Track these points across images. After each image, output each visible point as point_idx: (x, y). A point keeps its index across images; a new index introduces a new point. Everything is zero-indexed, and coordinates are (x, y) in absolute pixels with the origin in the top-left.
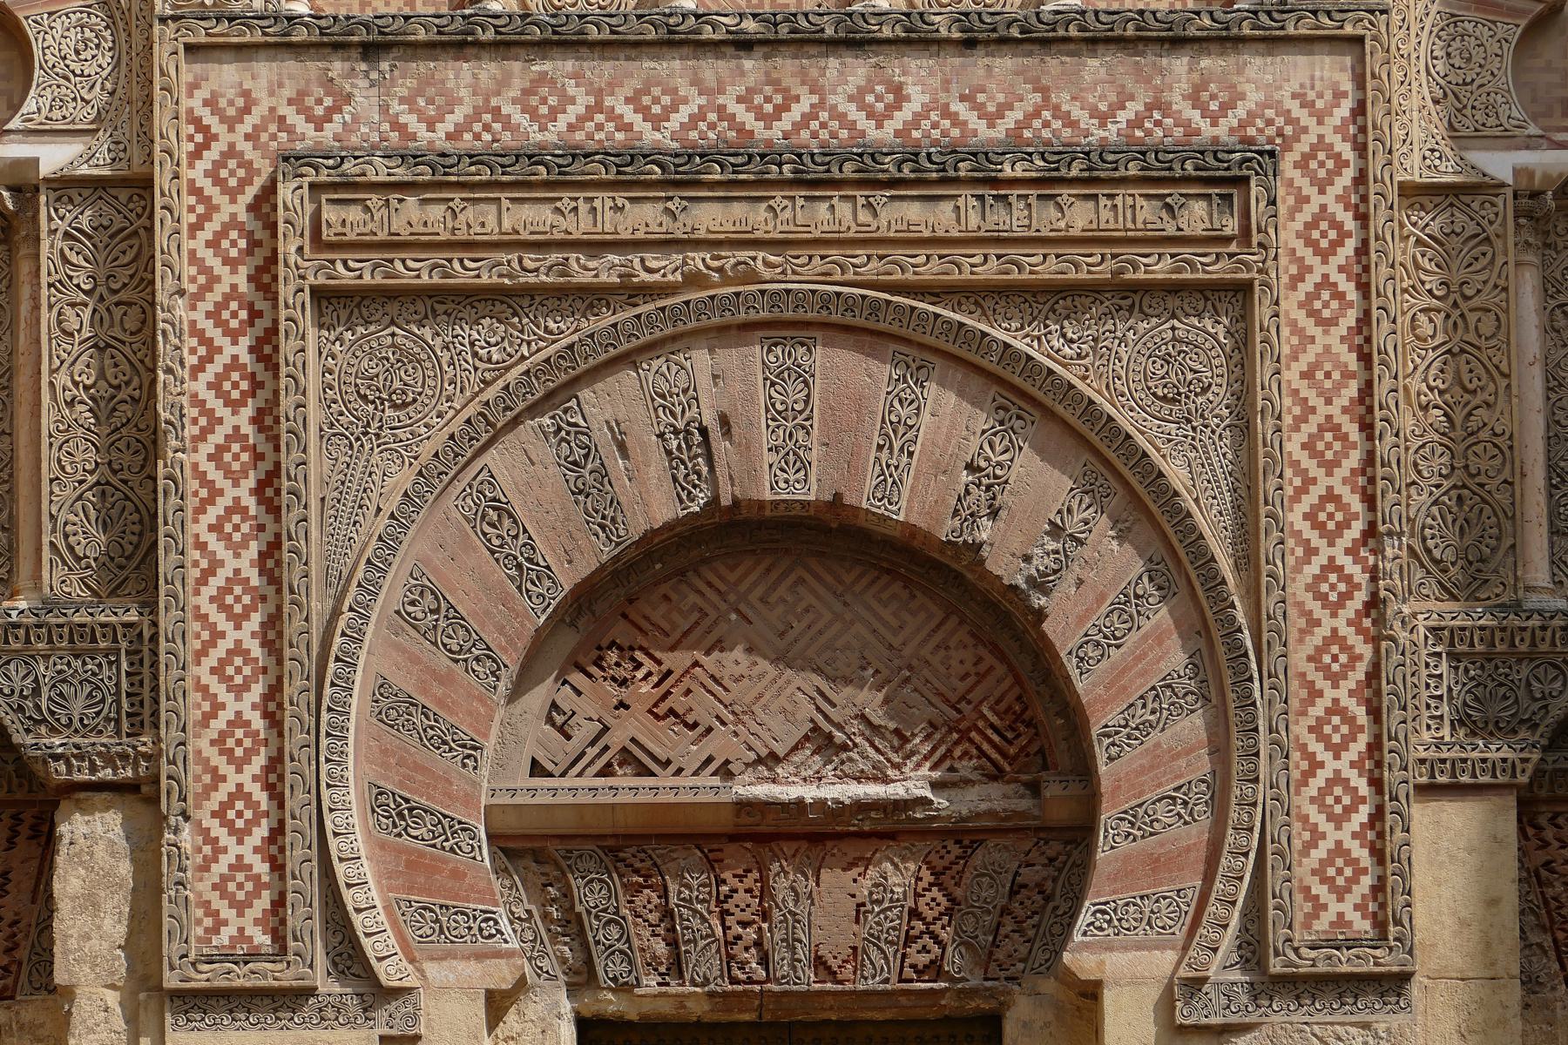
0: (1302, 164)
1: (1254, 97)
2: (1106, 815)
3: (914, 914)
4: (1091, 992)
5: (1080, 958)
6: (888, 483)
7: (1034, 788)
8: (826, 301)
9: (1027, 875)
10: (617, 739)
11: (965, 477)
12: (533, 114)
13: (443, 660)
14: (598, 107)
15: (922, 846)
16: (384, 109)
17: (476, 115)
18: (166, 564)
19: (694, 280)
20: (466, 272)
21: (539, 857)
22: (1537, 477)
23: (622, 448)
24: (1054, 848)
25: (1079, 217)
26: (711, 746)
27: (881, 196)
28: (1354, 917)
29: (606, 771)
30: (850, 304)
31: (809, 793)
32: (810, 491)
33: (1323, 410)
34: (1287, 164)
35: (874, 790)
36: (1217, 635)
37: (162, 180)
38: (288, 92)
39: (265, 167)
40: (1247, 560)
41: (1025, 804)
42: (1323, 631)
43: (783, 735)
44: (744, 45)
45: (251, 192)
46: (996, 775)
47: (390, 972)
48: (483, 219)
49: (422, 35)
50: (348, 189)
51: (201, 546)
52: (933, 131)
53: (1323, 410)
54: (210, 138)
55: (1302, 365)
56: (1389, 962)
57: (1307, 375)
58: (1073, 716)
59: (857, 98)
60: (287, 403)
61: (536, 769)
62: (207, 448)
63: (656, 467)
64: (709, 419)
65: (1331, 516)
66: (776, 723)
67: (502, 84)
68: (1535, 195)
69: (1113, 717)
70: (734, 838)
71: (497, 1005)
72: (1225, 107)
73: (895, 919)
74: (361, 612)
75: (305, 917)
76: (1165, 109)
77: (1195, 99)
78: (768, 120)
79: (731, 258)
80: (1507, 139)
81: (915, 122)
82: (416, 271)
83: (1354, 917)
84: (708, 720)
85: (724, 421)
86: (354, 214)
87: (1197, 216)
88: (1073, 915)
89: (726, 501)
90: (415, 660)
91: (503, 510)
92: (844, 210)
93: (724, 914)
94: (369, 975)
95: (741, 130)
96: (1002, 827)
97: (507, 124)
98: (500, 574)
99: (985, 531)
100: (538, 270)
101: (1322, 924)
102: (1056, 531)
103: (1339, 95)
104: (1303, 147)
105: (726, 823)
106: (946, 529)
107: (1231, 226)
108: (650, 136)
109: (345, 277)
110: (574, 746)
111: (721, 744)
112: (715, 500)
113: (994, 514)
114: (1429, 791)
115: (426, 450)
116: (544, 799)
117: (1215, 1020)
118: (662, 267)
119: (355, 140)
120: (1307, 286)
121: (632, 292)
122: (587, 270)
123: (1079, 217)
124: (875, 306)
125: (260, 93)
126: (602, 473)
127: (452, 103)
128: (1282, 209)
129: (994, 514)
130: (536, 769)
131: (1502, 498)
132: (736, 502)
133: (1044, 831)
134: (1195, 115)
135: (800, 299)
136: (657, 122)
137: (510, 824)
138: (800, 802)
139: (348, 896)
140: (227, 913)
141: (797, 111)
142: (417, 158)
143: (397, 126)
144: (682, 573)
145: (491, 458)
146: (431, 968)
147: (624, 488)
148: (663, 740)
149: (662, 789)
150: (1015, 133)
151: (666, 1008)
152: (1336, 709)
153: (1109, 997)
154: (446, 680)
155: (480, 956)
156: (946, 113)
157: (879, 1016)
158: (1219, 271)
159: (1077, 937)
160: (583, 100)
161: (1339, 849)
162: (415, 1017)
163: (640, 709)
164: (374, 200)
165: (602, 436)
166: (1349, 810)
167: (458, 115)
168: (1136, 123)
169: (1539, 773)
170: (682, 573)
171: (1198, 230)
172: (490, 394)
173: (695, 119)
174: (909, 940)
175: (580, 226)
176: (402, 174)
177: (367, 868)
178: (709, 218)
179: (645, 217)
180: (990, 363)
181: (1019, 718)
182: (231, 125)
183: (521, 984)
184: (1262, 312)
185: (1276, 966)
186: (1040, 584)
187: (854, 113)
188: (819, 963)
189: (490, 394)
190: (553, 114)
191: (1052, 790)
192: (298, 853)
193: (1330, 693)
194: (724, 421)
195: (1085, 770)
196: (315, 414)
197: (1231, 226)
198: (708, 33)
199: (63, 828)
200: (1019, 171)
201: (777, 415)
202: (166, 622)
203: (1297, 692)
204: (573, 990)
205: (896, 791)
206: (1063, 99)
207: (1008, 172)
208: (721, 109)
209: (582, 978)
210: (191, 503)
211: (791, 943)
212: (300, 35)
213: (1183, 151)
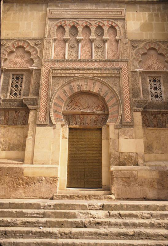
0: (123, 69)
1: (120, 65)
2: (110, 113)
3: (95, 120)
4: (108, 126)
5: (107, 123)
6: (93, 89)
7: (104, 111)
8: (89, 77)
9: (104, 118)
11: (99, 89)
15: (96, 115)
18: (40, 94)
19: (80, 76)
20: (63, 75)
21: (66, 115)
22: (141, 90)
23: (74, 87)
24: (106, 116)
25: (108, 72)
26: (80, 108)
27: (93, 71)
28: (129, 120)
29: (72, 109)
30: (91, 77)
31: (87, 111)
34: (122, 69)
36: (118, 100)
37: (42, 69)
39: (49, 68)
40: (120, 95)
41: (103, 112)
43: (85, 107)
44: (84, 61)
45: (48, 70)
46: (101, 110)
47: (54, 123)
48: (64, 72)
50: (55, 70)
51: (42, 93)
54: (46, 67)
56: (132, 124)
58: (107, 106)
60: (49, 83)
61: (66, 109)
62: (43, 86)
63: (76, 88)
64: (80, 85)
65: (126, 92)
68: (140, 72)
70: (81, 114)
71: (62, 126)
73: (93, 120)
74: (54, 97)
75: (48, 119)
76: (114, 66)
77: (116, 65)
79: (82, 74)
80: (138, 69)
81: (96, 66)
82: (59, 75)
83: (129, 120)
85: (81, 85)
86: (55, 71)
87: (116, 72)
88: (107, 119)
89: (81, 90)
91: (65, 91)
92: (90, 72)
93: (80, 120)
94: (52, 123)
96: (102, 114)
98: (64, 95)
100: (68, 75)
101: (127, 121)
102: (106, 93)
103: (126, 65)
104: (124, 68)
105: (81, 113)
107: (118, 73)
108: (77, 67)
109: (54, 75)
110: (69, 108)
112: (80, 90)
113: (101, 92)
114: (135, 111)
116: (67, 111)
117: (118, 128)
118: (77, 75)
120: (124, 77)
121: (75, 76)
122: (72, 75)
123: (108, 72)
124: (93, 78)
126: (72, 88)
127: (63, 65)
129: (101, 92)
130: (66, 109)
131: (139, 91)
132: (82, 91)
133: (105, 114)
135: (87, 77)
137: (64, 113)
138: (86, 112)
139: (51, 116)
140: (42, 118)
141: (87, 65)
142: (60, 68)
144: (78, 96)
145: (64, 87)
146: (57, 123)
147: (74, 89)
149: (76, 110)
150: (103, 67)
151: (75, 127)
152: (127, 105)
153: (110, 126)
155: (61, 122)
157: (92, 128)
158: (118, 76)
159: (107, 121)
160: (72, 65)
161: (128, 115)
162: (55, 126)
164: (57, 70)
165: (72, 86)
166: (128, 113)
167: (63, 65)
169: (143, 111)
170: (78, 96)
171: (116, 73)
174: (94, 122)
175: (71, 72)
176: (59, 69)
177: (53, 115)
178: (81, 72)
179: (76, 72)
181: (103, 106)
182: (47, 66)
183: (64, 124)
184: (121, 78)
185: (123, 124)
186: (105, 96)
188: (87, 124)
191: (106, 111)
192: (48, 114)
194: (81, 85)
195: (108, 110)
196: (51, 84)
197: (118, 73)
199: (30, 112)
201: (85, 85)
202: (39, 98)
203: (124, 104)
204: (68, 125)
205: (94, 111)
206: (106, 65)
209: (69, 125)
210: (42, 90)
211: (85, 122)
213: (115, 68)
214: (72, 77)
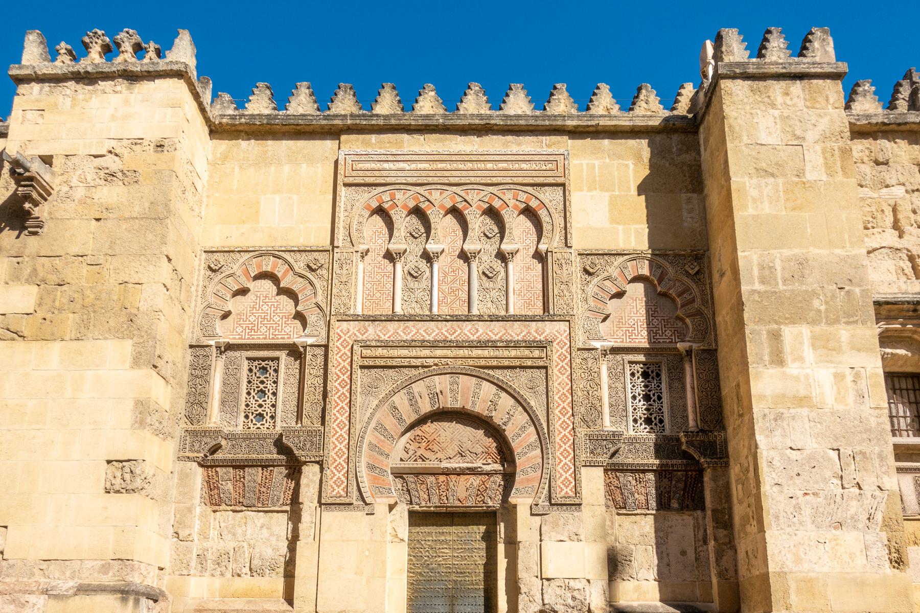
0: (558, 344)
1: (548, 331)
10: (418, 454)
12: (405, 333)
13: (382, 438)
14: (418, 332)
16: (375, 332)
17: (394, 333)
32: (458, 405)
33: (562, 391)
35: (470, 465)
38: (357, 329)
42: (563, 434)
49: (383, 319)
52: (484, 338)
53: (562, 391)
54: (341, 337)
55: (558, 382)
57: (559, 384)
59: (469, 331)
66: (451, 451)
67: (400, 327)
69: (519, 450)
72: (542, 333)
77: (536, 331)
78: (451, 335)
81: (481, 335)
84: (436, 450)
90: (377, 438)
95: (446, 337)
97: (400, 335)
99: (494, 414)
104: (558, 341)
106: (486, 413)
108: (427, 338)
111: (439, 455)
115: (381, 397)
119: (369, 338)
120: (559, 367)
125: (351, 329)
127: (389, 331)
128: (554, 352)
134: (536, 335)
136: (429, 335)
143: (378, 335)
148: (427, 454)
150: (501, 337)
154: (383, 441)
156: (487, 334)
160: (415, 331)
163: (423, 448)
168: (525, 336)
172: (394, 386)
173: (437, 335)
176: (378, 344)
178: (439, 352)
179: (426, 352)
180: (496, 381)
187: (468, 334)
189: (394, 386)
190: (409, 334)
193: (564, 447)
198: (440, 319)
200: (501, 345)
206: (510, 331)
207: (499, 345)
208: (442, 333)
212: (360, 318)
214: (416, 367)
